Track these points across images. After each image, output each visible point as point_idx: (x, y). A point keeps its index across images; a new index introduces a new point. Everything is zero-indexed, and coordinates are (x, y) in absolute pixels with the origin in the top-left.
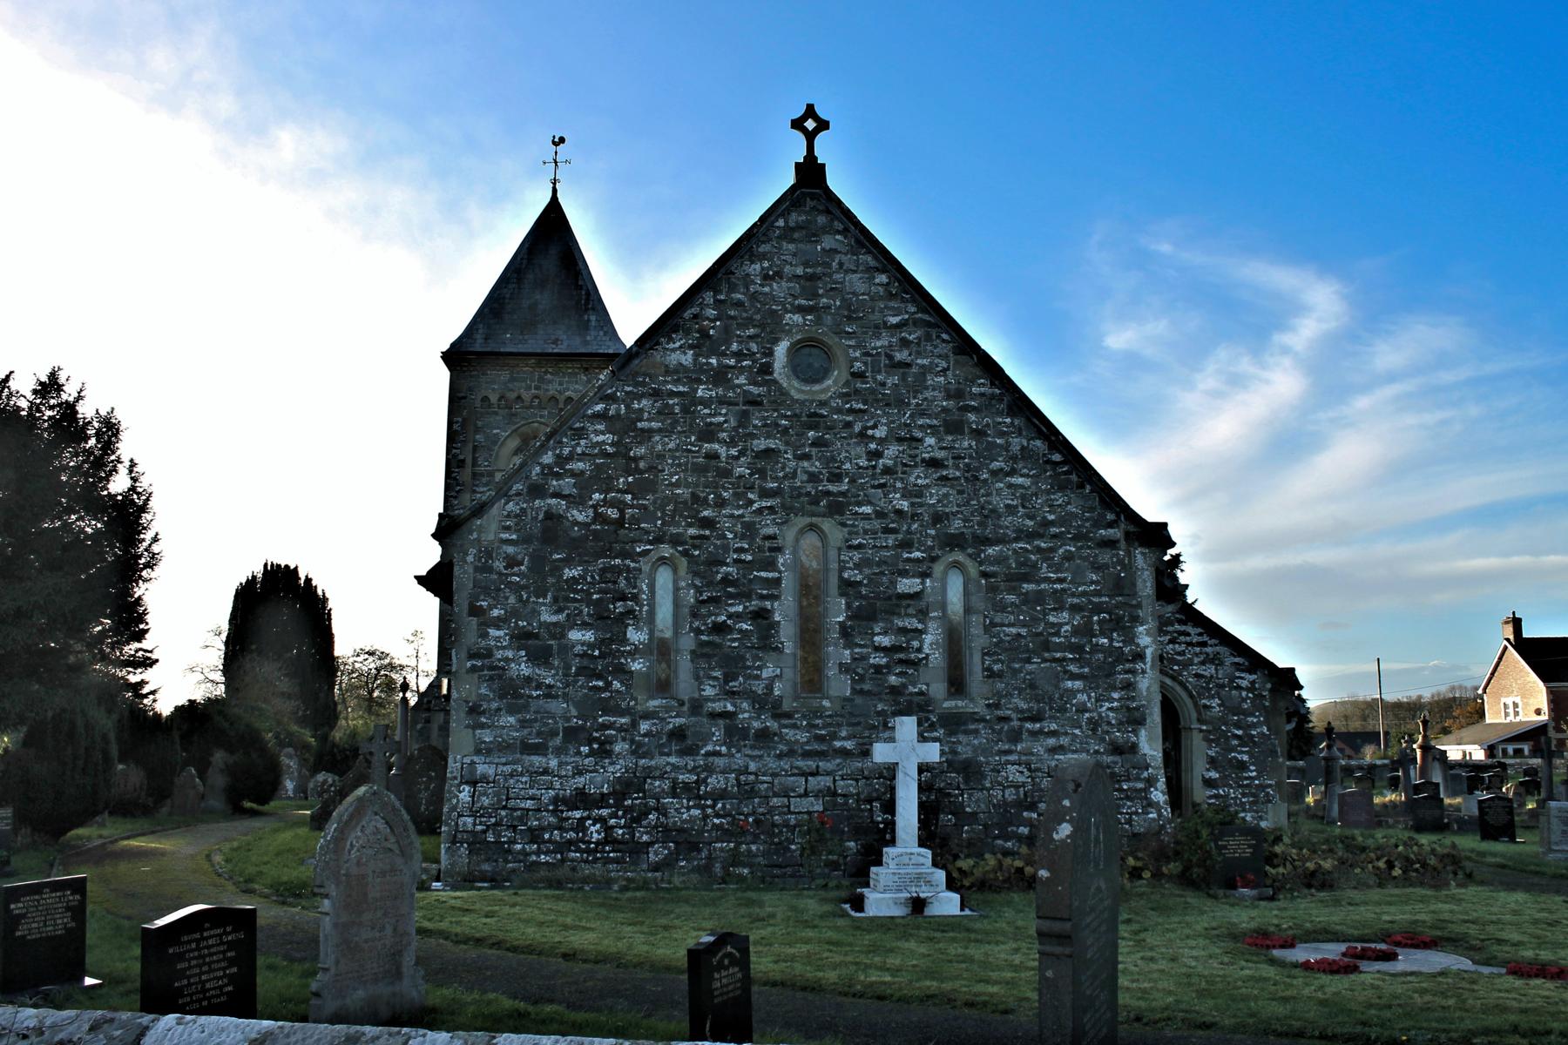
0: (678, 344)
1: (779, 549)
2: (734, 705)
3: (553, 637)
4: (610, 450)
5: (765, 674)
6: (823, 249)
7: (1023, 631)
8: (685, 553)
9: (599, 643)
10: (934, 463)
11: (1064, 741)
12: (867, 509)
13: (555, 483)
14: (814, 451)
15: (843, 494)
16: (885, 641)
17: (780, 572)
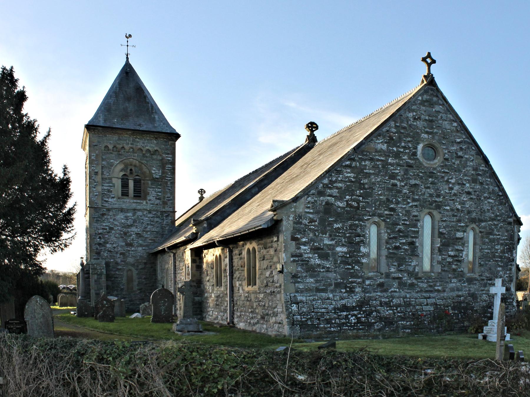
0: (381, 141)
1: (418, 220)
2: (401, 275)
3: (330, 249)
4: (353, 180)
5: (413, 264)
6: (435, 111)
7: (489, 251)
8: (384, 220)
9: (349, 252)
10: (469, 193)
12: (448, 208)
13: (329, 191)
14: (431, 186)
15: (441, 202)
16: (452, 253)
17: (419, 229)
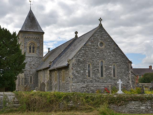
8: (91, 63)
9: (84, 72)
10: (112, 55)
11: (123, 81)
12: (107, 59)
15: (105, 58)
16: (108, 72)
